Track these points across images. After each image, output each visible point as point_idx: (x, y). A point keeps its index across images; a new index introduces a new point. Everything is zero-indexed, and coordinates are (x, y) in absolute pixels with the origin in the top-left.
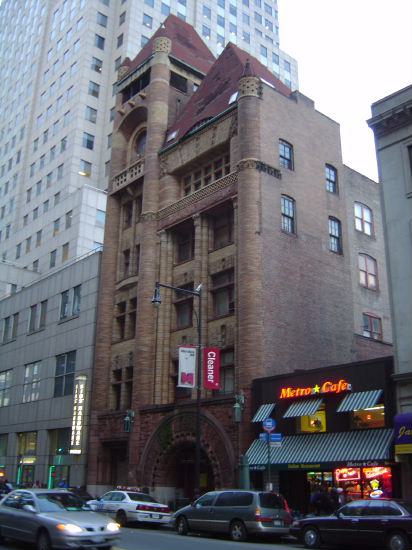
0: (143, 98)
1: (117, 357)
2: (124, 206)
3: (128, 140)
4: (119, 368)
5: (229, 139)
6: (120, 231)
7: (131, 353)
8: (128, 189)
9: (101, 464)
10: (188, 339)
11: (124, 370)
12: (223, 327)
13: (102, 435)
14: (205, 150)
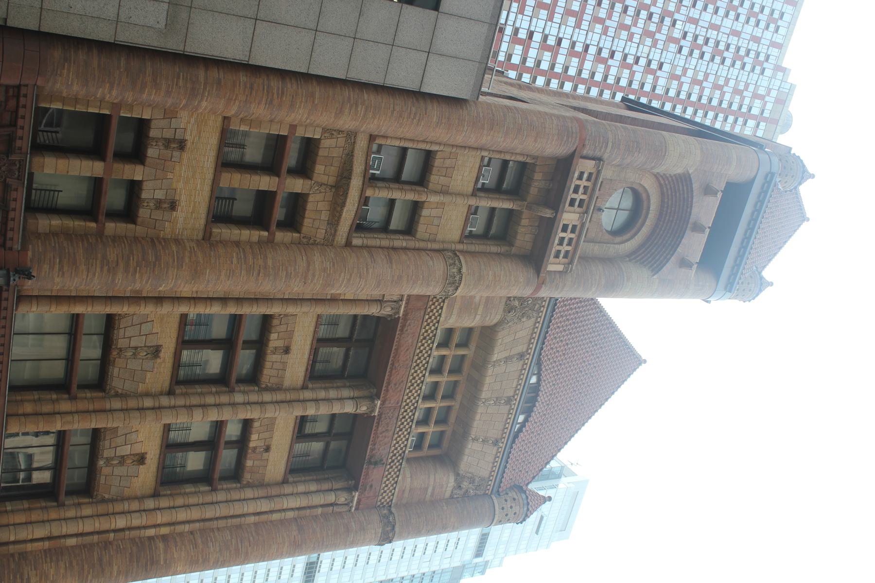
0: (684, 263)
1: (182, 145)
2: (534, 165)
5: (457, 475)
7: (173, 206)
8: (548, 213)
11: (136, 172)
12: (141, 459)
14: (475, 424)
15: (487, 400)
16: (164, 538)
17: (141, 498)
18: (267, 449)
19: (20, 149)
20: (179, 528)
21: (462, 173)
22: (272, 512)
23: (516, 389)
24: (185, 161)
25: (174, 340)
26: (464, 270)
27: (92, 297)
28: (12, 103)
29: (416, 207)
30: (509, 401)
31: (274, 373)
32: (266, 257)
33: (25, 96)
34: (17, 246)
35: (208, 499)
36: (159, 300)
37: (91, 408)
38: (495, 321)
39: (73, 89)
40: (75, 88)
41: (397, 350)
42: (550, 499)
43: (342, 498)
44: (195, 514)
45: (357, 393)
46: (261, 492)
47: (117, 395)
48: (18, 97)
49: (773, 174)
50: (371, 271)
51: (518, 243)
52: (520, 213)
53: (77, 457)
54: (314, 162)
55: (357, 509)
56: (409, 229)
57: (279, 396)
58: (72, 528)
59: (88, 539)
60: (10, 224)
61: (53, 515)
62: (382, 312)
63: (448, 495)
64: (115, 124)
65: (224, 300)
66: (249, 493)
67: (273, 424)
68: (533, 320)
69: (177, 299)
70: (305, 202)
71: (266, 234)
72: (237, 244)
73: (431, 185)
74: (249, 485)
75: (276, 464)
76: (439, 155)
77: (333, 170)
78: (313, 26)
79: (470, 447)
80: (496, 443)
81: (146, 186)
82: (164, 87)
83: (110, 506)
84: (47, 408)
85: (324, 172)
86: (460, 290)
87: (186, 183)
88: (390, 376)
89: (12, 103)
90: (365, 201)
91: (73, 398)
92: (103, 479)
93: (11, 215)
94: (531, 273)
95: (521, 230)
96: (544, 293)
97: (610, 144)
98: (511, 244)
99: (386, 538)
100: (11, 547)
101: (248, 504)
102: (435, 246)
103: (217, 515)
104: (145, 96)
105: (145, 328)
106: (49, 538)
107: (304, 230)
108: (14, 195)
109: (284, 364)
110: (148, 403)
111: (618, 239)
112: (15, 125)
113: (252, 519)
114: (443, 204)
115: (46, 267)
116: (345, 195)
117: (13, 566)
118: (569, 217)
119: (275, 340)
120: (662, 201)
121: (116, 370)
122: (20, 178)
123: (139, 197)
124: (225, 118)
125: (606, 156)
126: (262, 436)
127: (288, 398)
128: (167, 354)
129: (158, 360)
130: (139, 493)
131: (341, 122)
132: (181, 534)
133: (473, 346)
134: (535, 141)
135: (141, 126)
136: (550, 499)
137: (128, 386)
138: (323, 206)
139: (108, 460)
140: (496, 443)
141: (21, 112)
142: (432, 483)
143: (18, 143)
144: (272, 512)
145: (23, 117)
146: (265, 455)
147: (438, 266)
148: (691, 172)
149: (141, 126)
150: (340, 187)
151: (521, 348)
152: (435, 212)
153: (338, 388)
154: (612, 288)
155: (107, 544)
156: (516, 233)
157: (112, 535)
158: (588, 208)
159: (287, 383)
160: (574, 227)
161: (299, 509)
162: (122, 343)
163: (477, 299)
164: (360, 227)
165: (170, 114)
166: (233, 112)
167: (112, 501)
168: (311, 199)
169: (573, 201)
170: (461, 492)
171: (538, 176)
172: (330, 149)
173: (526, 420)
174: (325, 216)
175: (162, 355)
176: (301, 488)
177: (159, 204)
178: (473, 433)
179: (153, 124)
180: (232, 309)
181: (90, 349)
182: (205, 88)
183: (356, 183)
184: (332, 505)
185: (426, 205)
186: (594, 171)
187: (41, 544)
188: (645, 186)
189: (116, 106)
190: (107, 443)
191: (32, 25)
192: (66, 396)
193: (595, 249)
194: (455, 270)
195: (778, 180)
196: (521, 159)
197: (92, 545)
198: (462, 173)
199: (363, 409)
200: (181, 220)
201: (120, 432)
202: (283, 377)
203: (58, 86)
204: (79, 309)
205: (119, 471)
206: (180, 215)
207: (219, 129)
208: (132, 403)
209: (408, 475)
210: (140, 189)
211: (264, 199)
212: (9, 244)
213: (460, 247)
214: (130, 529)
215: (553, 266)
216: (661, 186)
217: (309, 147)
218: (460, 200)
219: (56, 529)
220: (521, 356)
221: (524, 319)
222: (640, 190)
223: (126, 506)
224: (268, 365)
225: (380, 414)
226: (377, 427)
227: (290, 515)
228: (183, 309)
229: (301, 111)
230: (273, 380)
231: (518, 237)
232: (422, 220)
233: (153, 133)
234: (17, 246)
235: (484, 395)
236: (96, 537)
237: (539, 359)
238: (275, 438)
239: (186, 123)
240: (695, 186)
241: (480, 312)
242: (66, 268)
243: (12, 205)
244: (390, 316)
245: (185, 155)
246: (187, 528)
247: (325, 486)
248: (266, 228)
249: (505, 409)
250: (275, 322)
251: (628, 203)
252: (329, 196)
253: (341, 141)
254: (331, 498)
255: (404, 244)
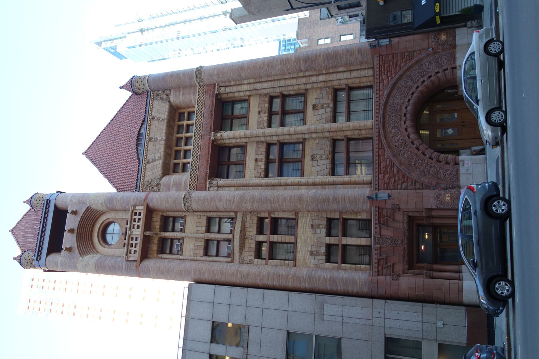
0: (75, 213)
1: (312, 253)
2: (158, 254)
3: (98, 252)
4: (323, 249)
5: (169, 102)
6: (181, 257)
7: (312, 226)
8: (148, 233)
9: (435, 274)
10: (315, 152)
12: (314, 107)
13: (399, 268)
15: (161, 140)
16: (301, 71)
17: (313, 88)
18: (259, 112)
19: (376, 250)
20: (295, 75)
21: (191, 247)
22: (254, 83)
23: (148, 146)
24: (310, 246)
25: (305, 163)
26: (183, 205)
27: (341, 184)
28: (380, 268)
29: (208, 230)
30: (150, 140)
31: (261, 150)
32: (271, 207)
33: (375, 272)
34: (373, 208)
35: (283, 89)
36: (314, 184)
37: (338, 133)
38: (164, 179)
39: (357, 275)
40: (357, 277)
41: (207, 164)
42: (120, 88)
43: (222, 90)
44: (288, 82)
45: (223, 141)
46: (259, 92)
47: (327, 138)
48: (378, 271)
49: (37, 260)
50: (225, 203)
51: (159, 217)
52: (160, 231)
53: (342, 107)
54: (256, 248)
55: (215, 84)
56: (210, 220)
57: (257, 139)
58: (342, 76)
59: (334, 70)
60: (377, 218)
61: (350, 81)
62: (216, 181)
63: (172, 91)
64: (340, 261)
65: (286, 185)
66: (265, 91)
67: (258, 125)
68: (145, 180)
69: (306, 185)
70: (257, 231)
71: (272, 216)
72: (284, 211)
73: (203, 240)
74: (266, 95)
75: (255, 104)
76: (202, 255)
77: (247, 246)
78: (264, 310)
79: (166, 116)
80: (153, 118)
81: (324, 235)
82: (322, 280)
83: (326, 85)
84: (356, 132)
85: (251, 245)
86: (183, 195)
87: (309, 237)
88: (209, 151)
89: (380, 268)
90: (232, 232)
91: (346, 136)
92: (330, 98)
93: (377, 222)
94: (151, 205)
95: (159, 223)
96: (142, 195)
97: (124, 268)
98: (162, 216)
99: (199, 70)
100: (367, 67)
101: (267, 87)
102: (197, 213)
103: (278, 82)
104: (329, 275)
105: (318, 169)
106: (351, 71)
107: (256, 218)
108: (377, 230)
109: (257, 154)
110: (314, 135)
111: (110, 220)
112: (378, 259)
113: (263, 80)
114: (196, 233)
115: (362, 200)
116: (240, 237)
117: (366, 59)
118: (137, 233)
119: (262, 164)
120: (92, 240)
121: (329, 149)
122: (375, 237)
123: (327, 229)
124: (295, 266)
125: (125, 262)
126: (262, 119)
127: (253, 139)
128: (308, 158)
129: (311, 154)
130: (314, 90)
131: (247, 269)
132: (294, 73)
133: (172, 165)
134: (159, 267)
135: (328, 260)
136: (120, 88)
137: (323, 142)
138: (249, 229)
139: (328, 107)
140: (153, 118)
141: (376, 265)
142: (181, 97)
143: (376, 252)
144: (254, 83)
145: (375, 263)
146: (260, 110)
147: (195, 206)
148: (81, 258)
149: (328, 260)
150: (243, 239)
151: (149, 166)
152: (200, 228)
153: (231, 143)
154: (110, 199)
155: (326, 68)
156: (161, 222)
157: (324, 72)
158: (129, 237)
159: (255, 144)
160: (134, 228)
161: (242, 84)
162: (327, 162)
163: (174, 189)
164: (233, 220)
165: (318, 266)
166: (292, 270)
167: (325, 87)
168: (255, 233)
169: (137, 239)
170: (166, 92)
171: (155, 249)
172: (250, 255)
173: (140, 130)
174: (248, 225)
175: (310, 157)
176: (242, 94)
177: (318, 227)
178: (165, 124)
179: (324, 261)
180: (283, 180)
181: (341, 157)
182: (305, 280)
183: (237, 241)
184: (227, 86)
185: (204, 232)
186: (129, 255)
187: (354, 68)
188: (102, 247)
189: (339, 268)
190: (329, 115)
191: (376, 301)
192: (349, 137)
193: (120, 215)
194: (187, 205)
195: (33, 257)
196: (164, 256)
197: (332, 68)
198: (191, 247)
199: (219, 135)
200: (308, 220)
201: (324, 120)
202: (257, 147)
203: (363, 277)
204: (347, 178)
205: (323, 101)
206: (309, 223)
207: (297, 261)
208: (321, 135)
209: (193, 101)
210: (326, 233)
211: (274, 231)
212: (377, 209)
213: (186, 214)
214: (317, 75)
215: (141, 209)
216: (94, 248)
217: (258, 255)
218: (189, 235)
219: (348, 75)
220: (148, 163)
221: (150, 180)
222: (104, 245)
223: (319, 85)
224: (264, 153)
225: (210, 132)
226: (211, 126)
227: (245, 82)
228: (303, 180)
229: (265, 273)
230: (261, 146)
231: (159, 220)
232: (205, 224)
233: (324, 257)
234: (373, 208)
235: (163, 143)
236: (331, 71)
237: (139, 161)
238: (257, 118)
239: (311, 262)
240: (77, 251)
241: (172, 183)
242: (354, 200)
243: (377, 226)
244: (212, 180)
245: (310, 248)
246: (292, 76)
247: (231, 95)
248: (272, 217)
249: (152, 135)
250: (263, 173)
251: (109, 238)
252: (247, 234)
253: (245, 259)
254: (228, 90)
255: (211, 214)
